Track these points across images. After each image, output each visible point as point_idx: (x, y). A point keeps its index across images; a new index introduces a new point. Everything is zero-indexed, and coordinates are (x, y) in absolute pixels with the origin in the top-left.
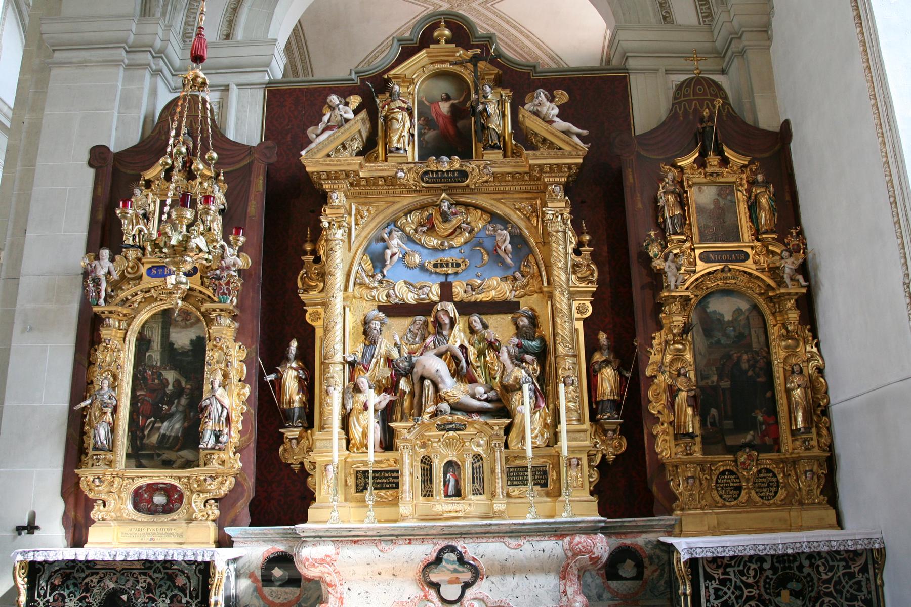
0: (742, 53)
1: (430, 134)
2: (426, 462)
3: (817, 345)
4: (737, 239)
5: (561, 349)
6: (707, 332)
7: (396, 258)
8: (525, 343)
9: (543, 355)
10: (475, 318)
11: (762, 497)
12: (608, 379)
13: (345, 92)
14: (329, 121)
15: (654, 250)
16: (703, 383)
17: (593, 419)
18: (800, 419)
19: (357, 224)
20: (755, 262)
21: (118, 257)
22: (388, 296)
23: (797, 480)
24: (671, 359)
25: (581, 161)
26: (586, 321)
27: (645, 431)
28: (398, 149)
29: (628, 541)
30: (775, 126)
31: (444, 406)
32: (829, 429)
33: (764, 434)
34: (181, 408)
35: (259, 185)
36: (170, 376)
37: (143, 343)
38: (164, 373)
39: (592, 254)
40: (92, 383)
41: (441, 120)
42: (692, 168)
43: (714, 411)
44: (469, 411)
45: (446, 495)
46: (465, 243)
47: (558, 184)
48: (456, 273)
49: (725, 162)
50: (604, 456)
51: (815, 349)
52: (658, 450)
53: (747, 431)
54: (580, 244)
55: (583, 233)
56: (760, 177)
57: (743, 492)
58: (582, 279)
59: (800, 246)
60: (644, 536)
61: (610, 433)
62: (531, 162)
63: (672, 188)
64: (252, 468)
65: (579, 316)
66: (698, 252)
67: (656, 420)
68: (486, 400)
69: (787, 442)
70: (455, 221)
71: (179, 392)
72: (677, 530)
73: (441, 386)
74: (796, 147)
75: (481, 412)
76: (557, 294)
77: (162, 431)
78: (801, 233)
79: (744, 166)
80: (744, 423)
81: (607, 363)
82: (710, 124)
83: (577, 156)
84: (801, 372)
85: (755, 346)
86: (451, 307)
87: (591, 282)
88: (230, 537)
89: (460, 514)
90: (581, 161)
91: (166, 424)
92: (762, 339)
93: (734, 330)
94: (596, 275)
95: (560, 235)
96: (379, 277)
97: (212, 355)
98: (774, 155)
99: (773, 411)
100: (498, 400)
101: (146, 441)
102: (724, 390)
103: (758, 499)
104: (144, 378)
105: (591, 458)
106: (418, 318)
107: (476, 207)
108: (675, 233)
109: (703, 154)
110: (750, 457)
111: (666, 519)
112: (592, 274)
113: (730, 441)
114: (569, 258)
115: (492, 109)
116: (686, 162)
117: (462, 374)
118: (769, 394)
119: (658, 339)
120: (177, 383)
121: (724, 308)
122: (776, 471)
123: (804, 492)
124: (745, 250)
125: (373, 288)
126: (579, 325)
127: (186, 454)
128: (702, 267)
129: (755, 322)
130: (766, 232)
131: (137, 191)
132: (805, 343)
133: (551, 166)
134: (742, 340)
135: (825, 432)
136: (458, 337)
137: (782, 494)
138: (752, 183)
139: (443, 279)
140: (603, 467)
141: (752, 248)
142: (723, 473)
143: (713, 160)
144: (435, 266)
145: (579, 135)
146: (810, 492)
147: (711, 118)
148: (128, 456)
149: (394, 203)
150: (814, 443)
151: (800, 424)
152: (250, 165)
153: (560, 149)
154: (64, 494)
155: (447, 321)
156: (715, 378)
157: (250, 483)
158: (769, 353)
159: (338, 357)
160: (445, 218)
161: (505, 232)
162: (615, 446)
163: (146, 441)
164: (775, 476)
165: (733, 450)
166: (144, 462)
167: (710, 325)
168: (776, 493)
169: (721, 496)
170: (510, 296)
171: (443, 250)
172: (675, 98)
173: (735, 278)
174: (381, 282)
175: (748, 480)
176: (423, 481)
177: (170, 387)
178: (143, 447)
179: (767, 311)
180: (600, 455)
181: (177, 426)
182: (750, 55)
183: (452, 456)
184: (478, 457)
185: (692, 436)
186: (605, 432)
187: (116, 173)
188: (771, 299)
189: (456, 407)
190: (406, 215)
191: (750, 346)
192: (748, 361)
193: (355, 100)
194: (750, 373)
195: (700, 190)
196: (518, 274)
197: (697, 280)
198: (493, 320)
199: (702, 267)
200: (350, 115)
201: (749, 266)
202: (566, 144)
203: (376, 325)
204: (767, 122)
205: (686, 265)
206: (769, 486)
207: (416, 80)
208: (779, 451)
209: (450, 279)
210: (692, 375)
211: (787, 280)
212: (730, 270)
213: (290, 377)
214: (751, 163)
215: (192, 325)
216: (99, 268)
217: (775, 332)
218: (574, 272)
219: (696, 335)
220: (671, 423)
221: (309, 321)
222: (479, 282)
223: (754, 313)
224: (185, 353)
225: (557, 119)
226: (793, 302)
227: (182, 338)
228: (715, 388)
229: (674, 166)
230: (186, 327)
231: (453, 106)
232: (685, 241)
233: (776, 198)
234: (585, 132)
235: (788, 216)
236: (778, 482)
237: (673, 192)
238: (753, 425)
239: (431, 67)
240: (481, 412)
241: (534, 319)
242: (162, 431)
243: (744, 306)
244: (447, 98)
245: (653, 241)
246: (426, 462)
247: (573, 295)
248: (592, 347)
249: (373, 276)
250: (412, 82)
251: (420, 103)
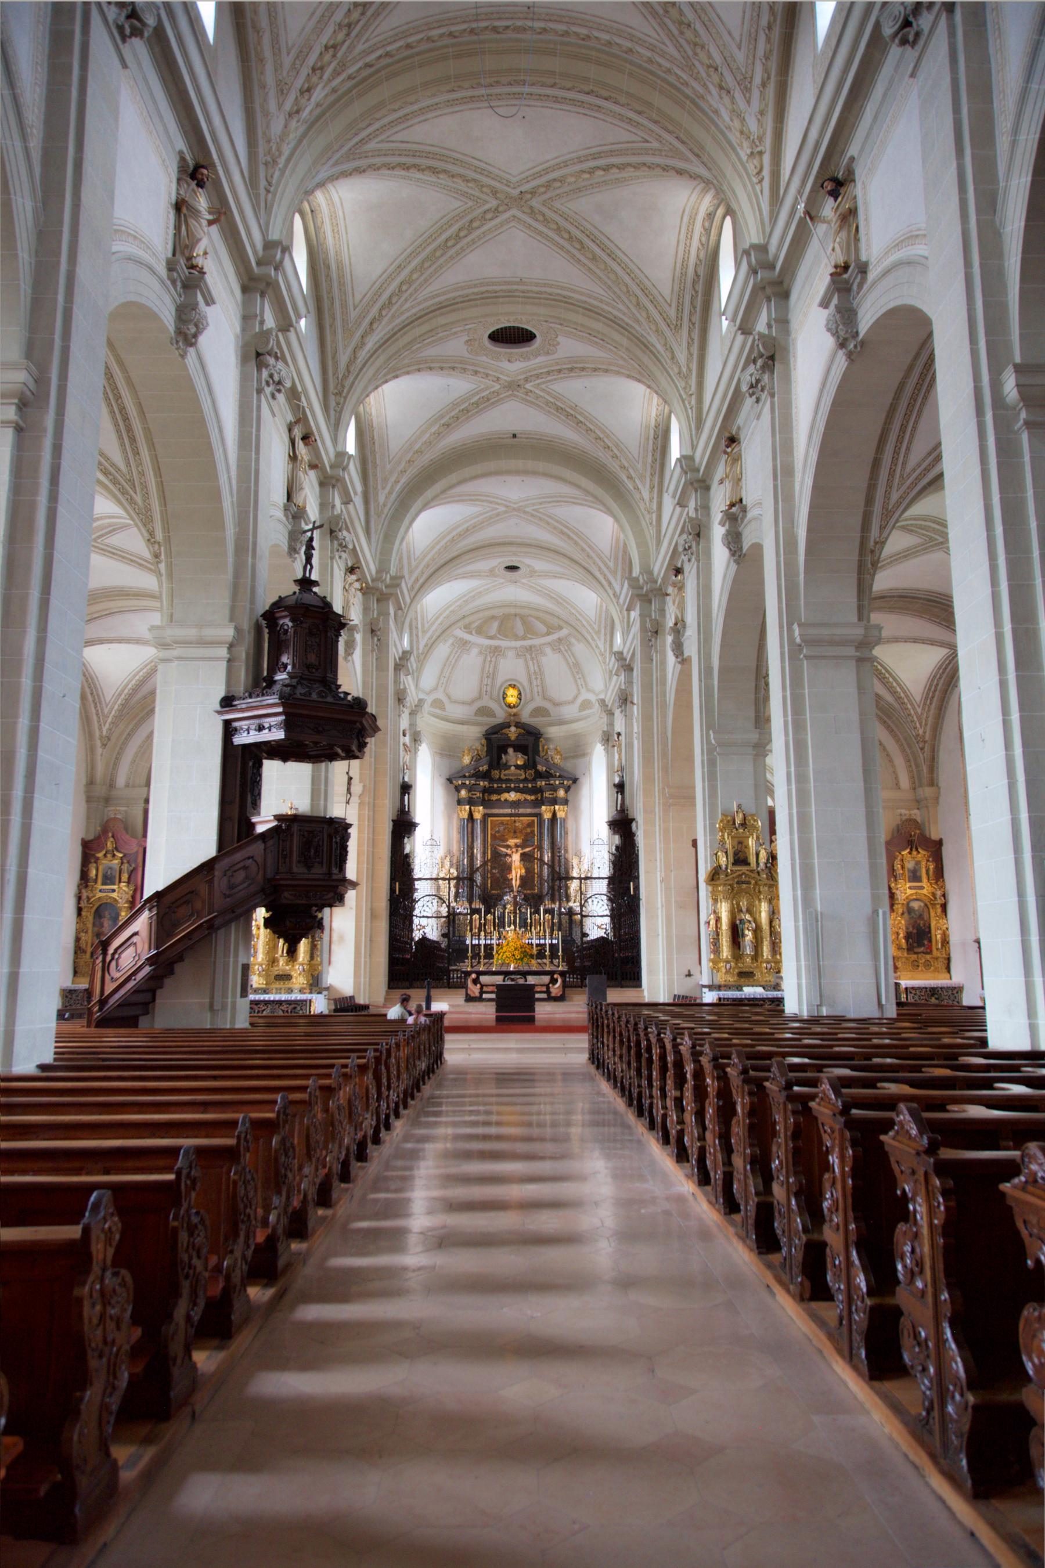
6: (909, 913)
59: (943, 887)
69: (935, 953)
74: (944, 848)
80: (920, 944)
98: (936, 849)
99: (930, 941)
113: (916, 950)
121: (915, 905)
128: (909, 892)
129: (926, 910)
134: (921, 916)
143: (914, 853)
167: (910, 910)
199: (909, 892)
201: (925, 891)
204: (934, 836)
217: (932, 914)
219: (906, 915)
233: (936, 867)
235: (939, 874)
238: (923, 945)
243: (922, 904)
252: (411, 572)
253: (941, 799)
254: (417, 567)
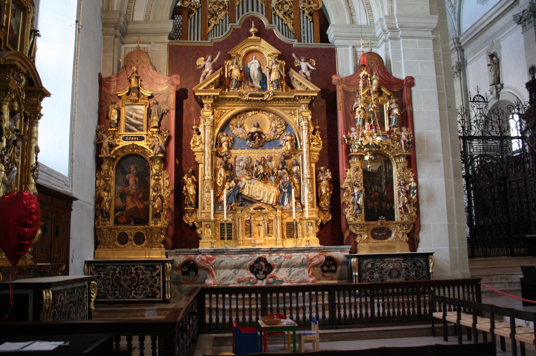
47: (307, 104)
50: (322, 221)
55: (316, 125)
62: (295, 94)
90: (316, 94)
105: (317, 221)
126: (313, 165)
140: (322, 226)
180: (320, 221)
186: (323, 211)
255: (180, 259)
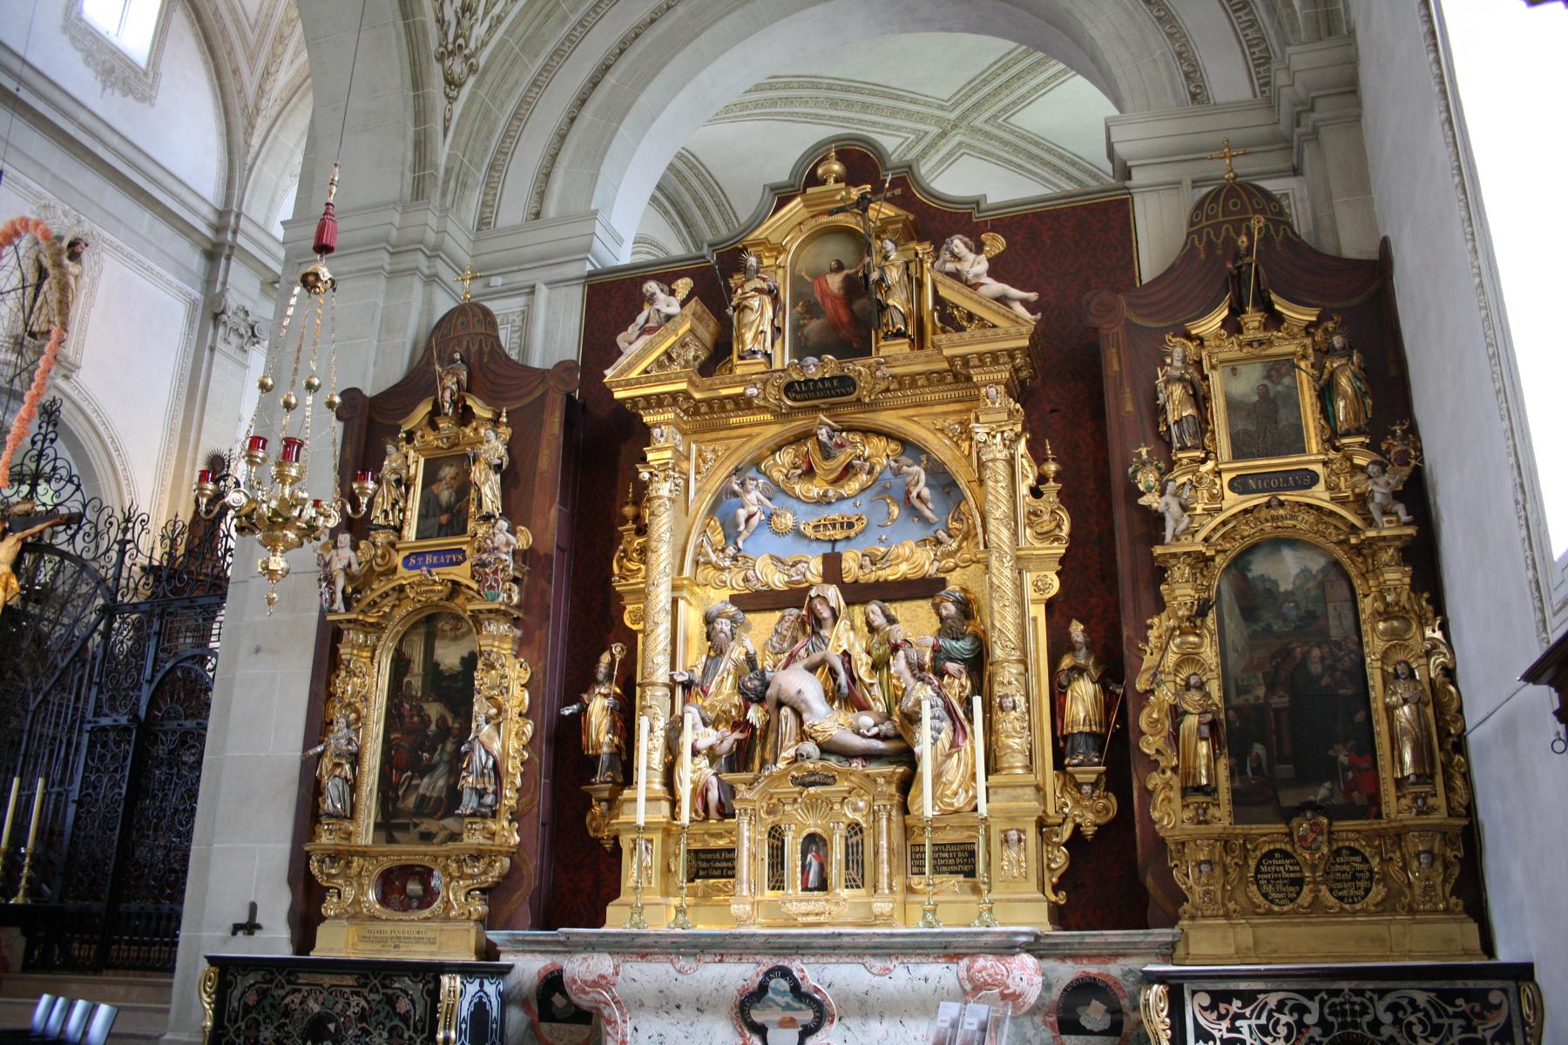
0: (1315, 134)
1: (814, 326)
2: (776, 834)
3: (1444, 627)
4: (1302, 450)
5: (998, 653)
6: (1249, 612)
7: (755, 521)
8: (947, 643)
9: (978, 664)
10: (874, 607)
11: (1341, 899)
12: (1083, 697)
13: (667, 279)
14: (647, 321)
15: (1147, 478)
16: (1236, 701)
17: (1059, 765)
18: (1408, 757)
19: (698, 472)
20: (1328, 488)
21: (362, 544)
22: (746, 580)
23: (1404, 868)
24: (1183, 661)
25: (1026, 343)
26: (1050, 605)
27: (1135, 785)
28: (754, 352)
29: (1093, 969)
30: (1370, 252)
31: (810, 747)
32: (1467, 777)
33: (1350, 787)
34: (446, 757)
35: (554, 425)
36: (434, 710)
37: (400, 665)
38: (425, 706)
39: (1059, 493)
40: (331, 723)
41: (828, 302)
42: (1218, 337)
43: (1258, 748)
44: (847, 754)
45: (805, 888)
46: (862, 490)
48: (848, 538)
49: (1274, 320)
50: (1077, 827)
51: (1438, 635)
52: (1155, 815)
53: (1319, 782)
54: (1042, 479)
55: (1046, 460)
56: (1337, 341)
57: (1306, 889)
58: (1042, 536)
60: (1121, 961)
61: (1087, 789)
62: (947, 352)
63: (1177, 373)
64: (535, 845)
65: (1036, 596)
66: (1226, 477)
67: (1154, 765)
68: (877, 736)
70: (842, 458)
71: (444, 732)
72: (1180, 951)
73: (805, 716)
75: (869, 756)
76: (994, 563)
77: (421, 790)
78: (1413, 430)
79: (1311, 324)
81: (1079, 671)
82: (1247, 260)
83: (1020, 336)
84: (1412, 675)
85: (1335, 633)
86: (833, 593)
87: (1058, 539)
88: (494, 945)
89: (822, 919)
90: (1026, 343)
91: (426, 780)
92: (1348, 622)
93: (1297, 607)
94: (1066, 527)
95: (1001, 468)
96: (731, 551)
97: (482, 679)
100: (898, 737)
101: (400, 805)
102: (1277, 711)
103: (1330, 900)
104: (401, 715)
106: (787, 611)
107: (879, 433)
108: (1183, 448)
109: (1237, 310)
110: (1315, 827)
111: (1161, 935)
112: (1059, 526)
114: (1020, 503)
115: (894, 275)
116: (1211, 324)
117: (846, 696)
118: (1360, 717)
119: (1159, 625)
120: (442, 718)
122: (1367, 852)
123: (1418, 891)
124: (1311, 467)
125: (723, 569)
126: (1038, 612)
127: (449, 823)
128: (1234, 502)
130: (1347, 434)
131: (390, 448)
132: (1422, 626)
133: (981, 356)
134: (1311, 624)
135: (1459, 782)
136: (845, 638)
137: (1378, 892)
138: (1325, 352)
139: (827, 549)
141: (1325, 463)
142: (1270, 855)
143: (1252, 319)
144: (816, 527)
145: (1025, 303)
146: (1428, 889)
147: (1249, 249)
148: (377, 826)
149: (751, 437)
150: (1440, 801)
151: (1409, 771)
152: (543, 397)
153: (994, 326)
154: (292, 881)
155: (826, 614)
156: (1261, 692)
157: (532, 866)
158: (1360, 643)
159: (662, 675)
160: (827, 455)
161: (916, 468)
162: (1089, 815)
163: (400, 805)
164: (1365, 860)
165: (1286, 815)
166: (397, 835)
167: (1252, 599)
168: (1368, 891)
169: (1265, 896)
170: (930, 569)
171: (829, 503)
172: (1192, 224)
173: (1293, 517)
174: (735, 558)
175: (1314, 868)
176: (771, 866)
177: (433, 727)
178: (397, 813)
179: (1353, 572)
181: (441, 783)
182: (1326, 135)
183: (813, 825)
184: (855, 828)
185: (1210, 790)
186: (1078, 786)
187: (371, 420)
188: (1357, 550)
189: (827, 749)
190: (773, 453)
191: (1324, 633)
192: (1322, 659)
193: (683, 286)
194: (1325, 681)
195: (1234, 371)
196: (942, 535)
197: (1224, 523)
198: (898, 609)
199: (1234, 502)
200: (674, 309)
201: (1319, 495)
202: (1008, 319)
203: (724, 625)
204: (1353, 244)
205: (1199, 500)
206: (1354, 878)
207: (787, 244)
208: (1379, 816)
209: (839, 548)
210: (1214, 688)
211: (1376, 514)
212: (1281, 504)
213: (599, 708)
214: (1321, 319)
215: (464, 636)
216: (335, 560)
217: (1367, 605)
218: (1031, 525)
220: (1174, 769)
221: (628, 623)
222: (883, 549)
223: (1333, 575)
224: (453, 677)
225: (989, 281)
226: (1391, 551)
227: (449, 656)
228: (1260, 709)
229: (1189, 337)
230: (456, 639)
231: (847, 279)
232: (1203, 461)
234: (1033, 296)
235: (1388, 405)
236: (1371, 871)
237: (1181, 379)
238: (1330, 771)
239: (812, 223)
240: (869, 756)
241: (966, 608)
242: (421, 790)
244: (840, 267)
245: (1144, 464)
246: (776, 834)
247: (1021, 564)
248: (1059, 645)
249: (723, 550)
250: (779, 249)
251: (797, 281)
252: (252, 58)
253: (1369, 77)
254: (260, 42)
255: (528, 967)
